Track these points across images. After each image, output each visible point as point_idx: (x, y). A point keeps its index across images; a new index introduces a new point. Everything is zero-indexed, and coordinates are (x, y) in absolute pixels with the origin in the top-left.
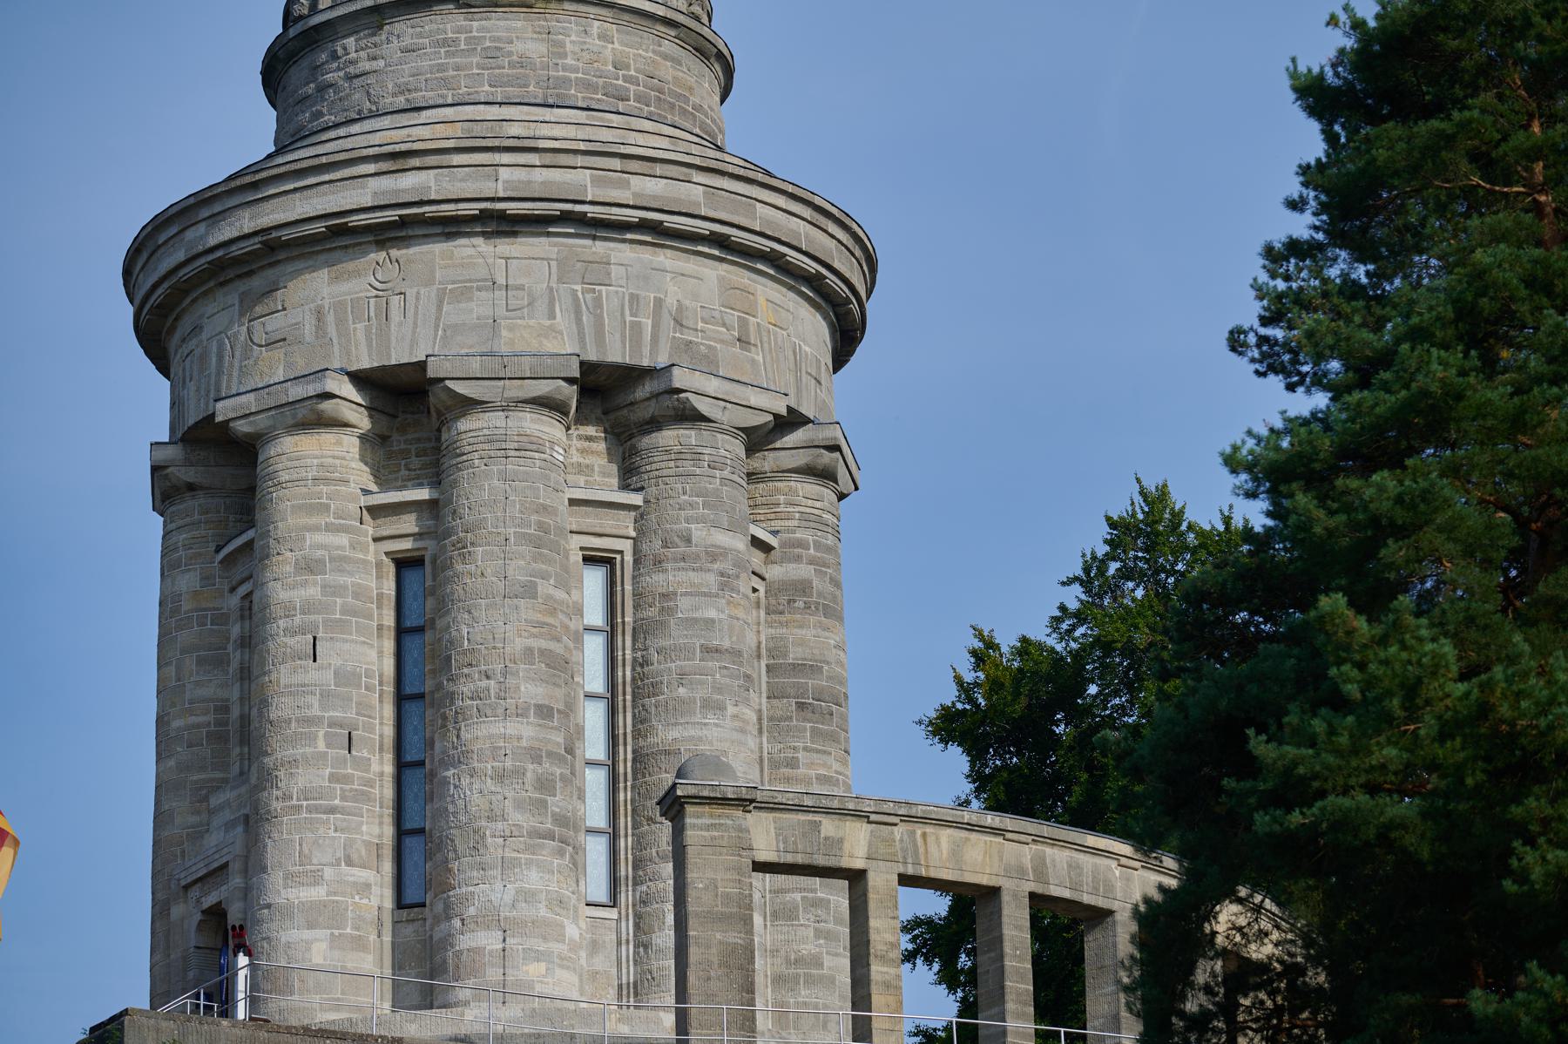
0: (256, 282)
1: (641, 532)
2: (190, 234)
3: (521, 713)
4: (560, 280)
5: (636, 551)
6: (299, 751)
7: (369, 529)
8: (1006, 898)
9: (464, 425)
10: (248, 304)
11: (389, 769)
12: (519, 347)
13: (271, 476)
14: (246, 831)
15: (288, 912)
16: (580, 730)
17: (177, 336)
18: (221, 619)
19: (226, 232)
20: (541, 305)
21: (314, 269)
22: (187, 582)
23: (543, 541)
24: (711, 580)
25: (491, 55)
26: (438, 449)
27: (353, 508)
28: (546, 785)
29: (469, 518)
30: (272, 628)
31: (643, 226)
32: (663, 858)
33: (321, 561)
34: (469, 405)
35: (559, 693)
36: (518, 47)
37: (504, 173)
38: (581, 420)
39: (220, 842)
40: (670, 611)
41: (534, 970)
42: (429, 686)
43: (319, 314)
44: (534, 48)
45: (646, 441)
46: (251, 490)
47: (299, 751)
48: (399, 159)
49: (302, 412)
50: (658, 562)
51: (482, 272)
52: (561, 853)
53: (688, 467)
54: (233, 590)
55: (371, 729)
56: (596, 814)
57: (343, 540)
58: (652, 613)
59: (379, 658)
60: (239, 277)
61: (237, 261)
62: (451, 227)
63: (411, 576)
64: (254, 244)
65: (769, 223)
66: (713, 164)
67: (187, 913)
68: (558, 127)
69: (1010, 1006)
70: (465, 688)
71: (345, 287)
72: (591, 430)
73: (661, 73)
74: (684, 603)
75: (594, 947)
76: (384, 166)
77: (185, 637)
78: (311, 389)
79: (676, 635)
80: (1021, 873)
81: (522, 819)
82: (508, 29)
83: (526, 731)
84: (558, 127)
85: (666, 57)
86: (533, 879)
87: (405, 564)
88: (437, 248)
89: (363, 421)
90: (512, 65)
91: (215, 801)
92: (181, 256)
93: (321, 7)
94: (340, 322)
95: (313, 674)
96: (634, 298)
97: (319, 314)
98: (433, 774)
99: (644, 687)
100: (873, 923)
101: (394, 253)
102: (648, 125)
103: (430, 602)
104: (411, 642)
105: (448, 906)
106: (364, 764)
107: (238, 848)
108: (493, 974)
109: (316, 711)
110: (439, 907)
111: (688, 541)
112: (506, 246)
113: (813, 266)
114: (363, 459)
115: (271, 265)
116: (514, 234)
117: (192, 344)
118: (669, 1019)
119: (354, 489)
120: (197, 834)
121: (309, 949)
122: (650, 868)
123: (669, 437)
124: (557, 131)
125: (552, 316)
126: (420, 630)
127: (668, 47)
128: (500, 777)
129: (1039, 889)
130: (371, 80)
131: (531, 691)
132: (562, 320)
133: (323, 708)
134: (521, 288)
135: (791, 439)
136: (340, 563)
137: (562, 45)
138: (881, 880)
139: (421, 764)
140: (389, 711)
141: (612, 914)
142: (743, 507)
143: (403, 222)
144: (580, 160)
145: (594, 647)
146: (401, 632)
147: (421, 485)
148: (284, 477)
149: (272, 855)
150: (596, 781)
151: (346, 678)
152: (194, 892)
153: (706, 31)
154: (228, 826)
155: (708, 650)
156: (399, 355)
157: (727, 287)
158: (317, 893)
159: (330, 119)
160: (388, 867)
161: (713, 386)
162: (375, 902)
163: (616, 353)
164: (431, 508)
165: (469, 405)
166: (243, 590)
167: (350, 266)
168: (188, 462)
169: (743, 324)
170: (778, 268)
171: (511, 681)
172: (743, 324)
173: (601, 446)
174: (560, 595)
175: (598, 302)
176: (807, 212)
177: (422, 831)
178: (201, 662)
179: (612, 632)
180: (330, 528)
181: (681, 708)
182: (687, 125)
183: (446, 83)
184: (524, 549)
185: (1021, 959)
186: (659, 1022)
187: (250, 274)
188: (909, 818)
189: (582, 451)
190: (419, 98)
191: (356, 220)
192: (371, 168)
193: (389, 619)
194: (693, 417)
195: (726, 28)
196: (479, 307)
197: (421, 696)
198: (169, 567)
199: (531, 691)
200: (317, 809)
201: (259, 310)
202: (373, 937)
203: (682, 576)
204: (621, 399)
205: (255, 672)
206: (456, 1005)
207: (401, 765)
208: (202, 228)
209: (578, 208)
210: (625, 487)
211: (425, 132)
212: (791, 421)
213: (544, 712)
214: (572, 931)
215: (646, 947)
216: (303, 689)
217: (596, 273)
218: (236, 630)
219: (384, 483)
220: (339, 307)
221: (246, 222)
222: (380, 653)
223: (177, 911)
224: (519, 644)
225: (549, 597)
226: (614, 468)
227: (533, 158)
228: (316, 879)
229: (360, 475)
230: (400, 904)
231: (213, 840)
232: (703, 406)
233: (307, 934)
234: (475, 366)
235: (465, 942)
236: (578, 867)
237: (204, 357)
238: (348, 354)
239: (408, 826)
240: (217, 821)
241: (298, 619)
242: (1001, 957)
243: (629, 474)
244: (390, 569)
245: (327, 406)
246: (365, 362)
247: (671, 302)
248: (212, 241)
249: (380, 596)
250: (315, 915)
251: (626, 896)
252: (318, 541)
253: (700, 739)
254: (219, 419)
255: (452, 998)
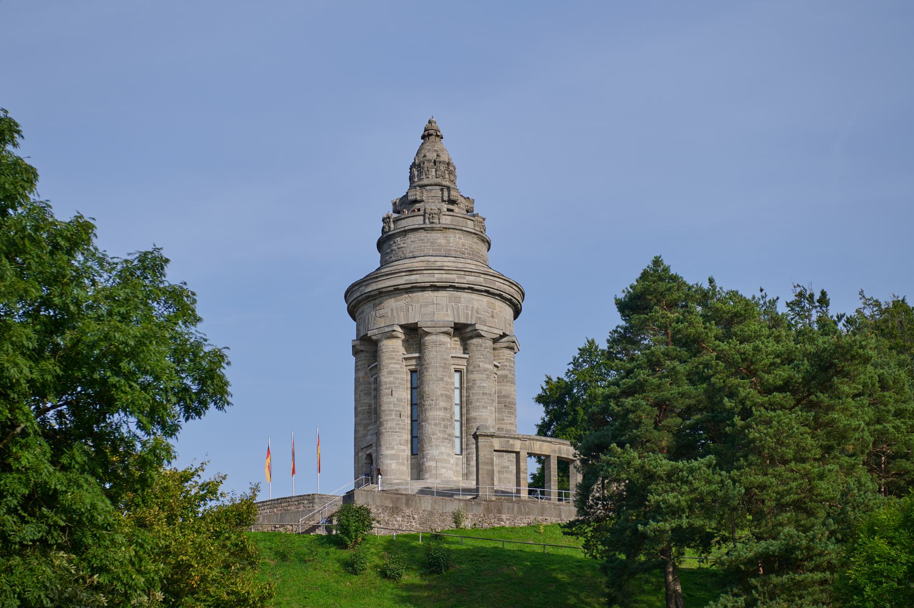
0: (377, 301)
1: (468, 364)
2: (361, 289)
3: (440, 409)
4: (449, 302)
5: (467, 369)
6: (388, 418)
7: (404, 363)
8: (552, 457)
9: (426, 338)
10: (375, 306)
11: (409, 422)
12: (439, 319)
13: (381, 350)
14: (376, 436)
15: (386, 456)
16: (454, 413)
17: (358, 313)
18: (369, 383)
19: (369, 289)
20: (445, 308)
21: (391, 298)
22: (361, 374)
23: (445, 367)
24: (485, 376)
25: (433, 243)
26: (420, 343)
27: (401, 358)
28: (446, 427)
29: (428, 362)
30: (382, 387)
31: (469, 288)
32: (473, 444)
33: (393, 371)
34: (427, 333)
35: (449, 404)
36: (439, 241)
37: (436, 275)
38: (454, 336)
39: (370, 438)
40: (475, 384)
41: (443, 471)
42: (418, 402)
43: (392, 310)
44: (443, 241)
45: (469, 342)
46: (376, 351)
47: (388, 418)
48: (411, 272)
49: (388, 335)
50: (472, 372)
51: (431, 300)
52: (449, 443)
53: (479, 348)
54: (372, 376)
55: (405, 412)
56: (457, 432)
57: (398, 366)
58: (470, 384)
59: (406, 395)
60: (373, 300)
61: (372, 296)
62: (423, 289)
63: (414, 375)
64: (376, 292)
65: (499, 287)
66: (486, 273)
67: (362, 455)
68: (448, 263)
69: (552, 483)
70: (427, 403)
71: (398, 303)
72: (456, 339)
73: (474, 247)
74: (478, 382)
75: (457, 465)
76: (407, 273)
77: (361, 388)
78: (391, 329)
79: (476, 390)
80: (555, 451)
81: (441, 435)
82: (437, 236)
83: (441, 414)
84: (448, 263)
85: (474, 243)
86: (443, 449)
87: (412, 372)
88: (420, 294)
89: (403, 337)
90: (437, 246)
91: (368, 428)
92: (359, 294)
93: (392, 229)
94: (397, 312)
95: (391, 399)
96: (467, 306)
97: (392, 310)
98: (419, 423)
99: (469, 402)
100: (521, 464)
101: (410, 295)
102: (470, 261)
103: (419, 381)
104: (414, 391)
105: (423, 456)
106: (404, 421)
107: (375, 440)
108: (434, 472)
109: (392, 408)
110: (421, 456)
111: (479, 367)
112: (437, 294)
113: (509, 297)
114: (403, 346)
115: (380, 297)
116: (438, 290)
117: (362, 315)
118: (474, 483)
119: (401, 353)
120: (365, 436)
121: (391, 465)
122: (470, 446)
123: (475, 341)
124: (449, 264)
125: (447, 311)
126: (417, 388)
127: (475, 240)
128: (435, 425)
129: (560, 455)
130: (404, 249)
131: (442, 404)
132: (450, 312)
133: (394, 407)
134: (440, 304)
135: (503, 340)
136: (398, 372)
137: (449, 240)
138: (523, 454)
139: (417, 420)
140: (409, 408)
141: (461, 457)
142: (492, 358)
143: (412, 287)
144: (454, 272)
145: (457, 392)
146: (412, 388)
147: (416, 353)
148: (384, 350)
149: (382, 443)
150: (457, 425)
151: (399, 400)
152: (364, 450)
153: (484, 236)
154: (372, 435)
155: (483, 394)
156: (411, 321)
157: (489, 303)
158: (393, 452)
159: (393, 258)
160: (409, 445)
161: (485, 328)
162: (406, 454)
163: (462, 321)
164: (419, 358)
165: (427, 333)
166: (375, 377)
167: (399, 298)
168: (361, 345)
169: (492, 312)
170: (501, 298)
171: (438, 401)
172: (492, 312)
173: (459, 343)
174: (449, 380)
175: (458, 307)
176: (508, 283)
177: (417, 437)
178: (365, 394)
179: (461, 389)
180: (395, 363)
181: (478, 408)
182: (479, 260)
183: (422, 250)
184: (441, 369)
185: (555, 472)
186: (472, 483)
187: (375, 299)
188: (530, 439)
189: (454, 344)
190: (416, 254)
191: (401, 287)
192: (404, 274)
193: (409, 386)
194: (480, 336)
195: (488, 234)
196: (430, 309)
197: (417, 404)
198: (357, 371)
199: (442, 404)
200: (393, 432)
201: (378, 308)
202: (406, 462)
203: (478, 375)
204: (463, 332)
205: (378, 398)
206: (425, 479)
207: (412, 421)
208: (364, 288)
209: (454, 284)
210: (464, 353)
211: (417, 264)
212: (505, 335)
213: (445, 409)
214: (452, 461)
215: (469, 465)
216: (389, 403)
217: (458, 300)
218: (373, 386)
219: (408, 351)
220: (397, 308)
221: (374, 287)
222: (407, 394)
223: (360, 454)
224: (439, 393)
225: (447, 381)
226: (462, 348)
227: (443, 272)
228: (393, 448)
229: (402, 350)
230: (412, 454)
231: (369, 437)
232: (483, 333)
233: (391, 462)
234: (429, 324)
235: (427, 464)
236: (453, 446)
237: (365, 319)
238: (399, 319)
239: (414, 435)
240: (370, 433)
241: (388, 386)
242: (550, 472)
243: (465, 350)
244: (409, 373)
245: (394, 333)
246: (403, 323)
247: (475, 307)
248: (366, 291)
249: (407, 380)
250: (393, 457)
251: (464, 453)
252: (393, 366)
253: (482, 415)
254: (369, 335)
255: (424, 477)
